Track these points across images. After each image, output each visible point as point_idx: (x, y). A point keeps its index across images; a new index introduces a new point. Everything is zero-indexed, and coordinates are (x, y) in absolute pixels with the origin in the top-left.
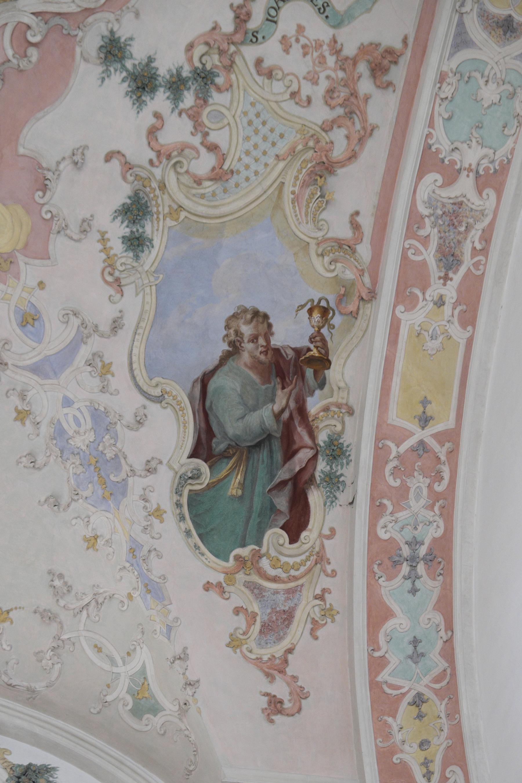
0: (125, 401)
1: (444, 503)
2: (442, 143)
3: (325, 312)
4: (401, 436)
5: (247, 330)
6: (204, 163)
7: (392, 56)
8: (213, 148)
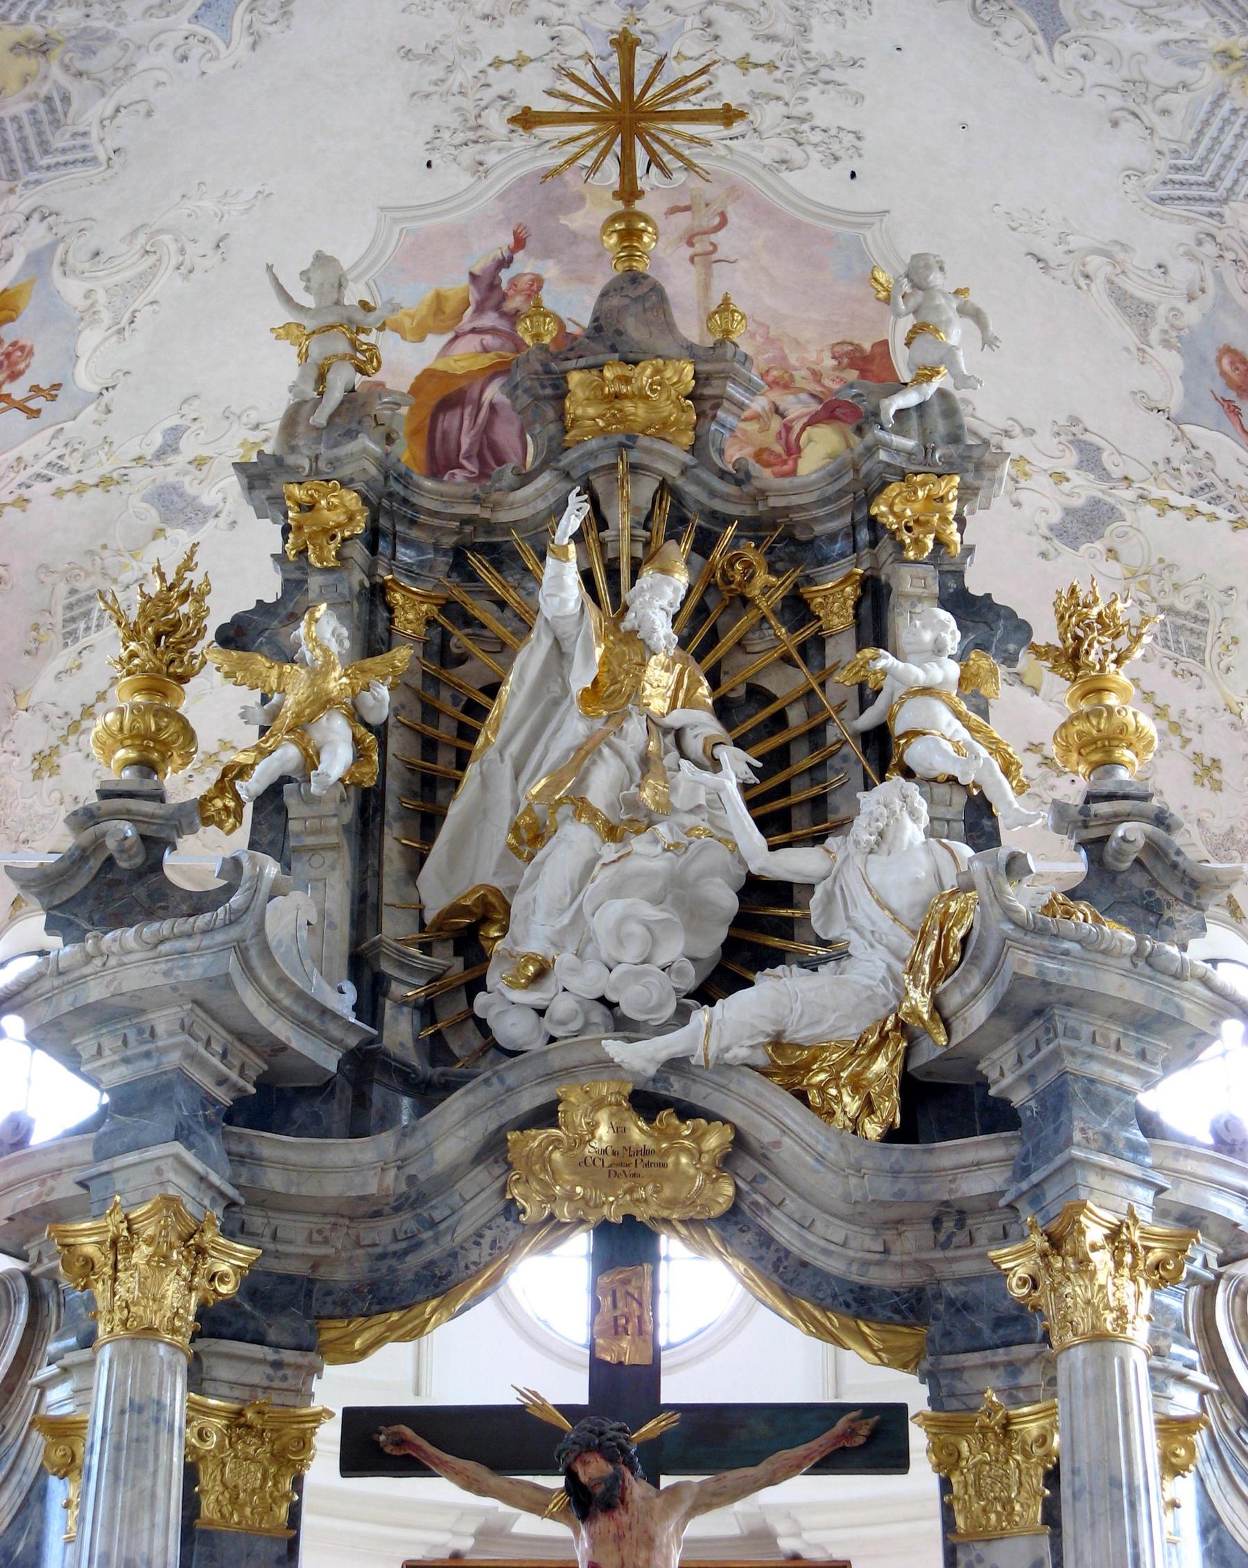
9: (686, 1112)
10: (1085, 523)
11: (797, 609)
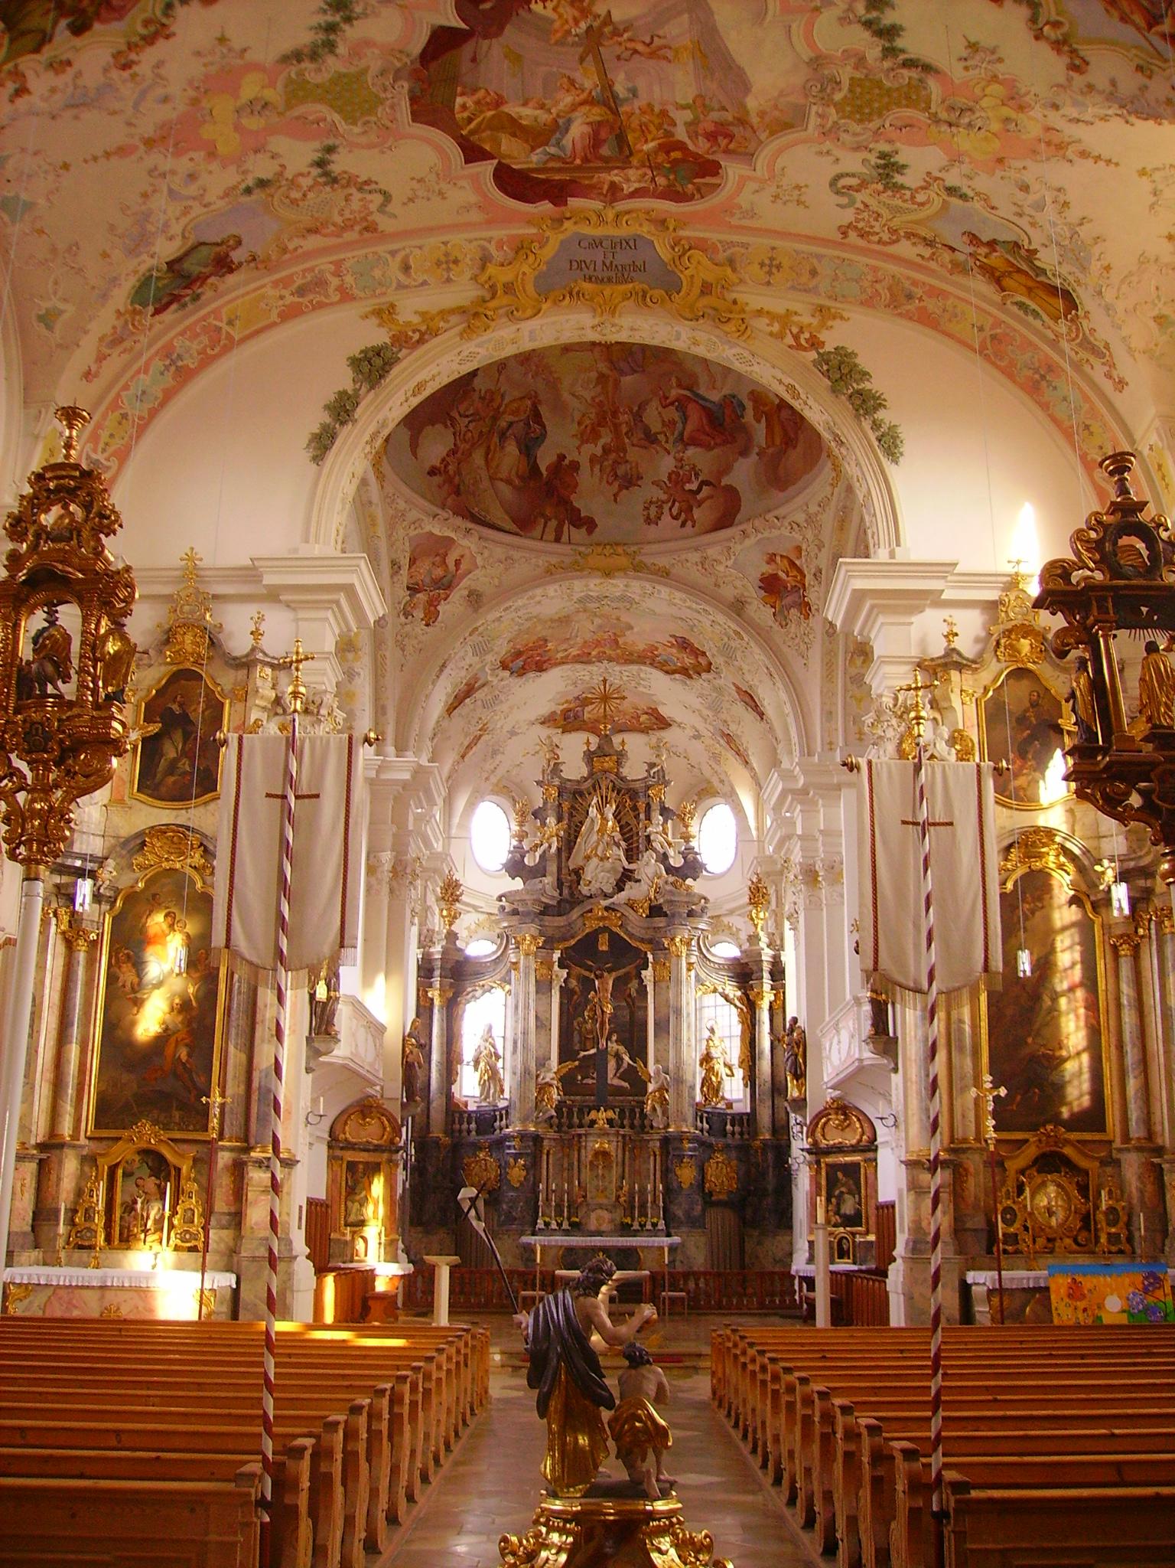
0: (176, 229)
1: (207, 361)
2: (347, 264)
3: (254, 259)
4: (219, 318)
5: (231, 242)
6: (296, 195)
7: (376, 230)
8: (305, 195)
9: (614, 910)
10: (697, 736)
11: (635, 808)
